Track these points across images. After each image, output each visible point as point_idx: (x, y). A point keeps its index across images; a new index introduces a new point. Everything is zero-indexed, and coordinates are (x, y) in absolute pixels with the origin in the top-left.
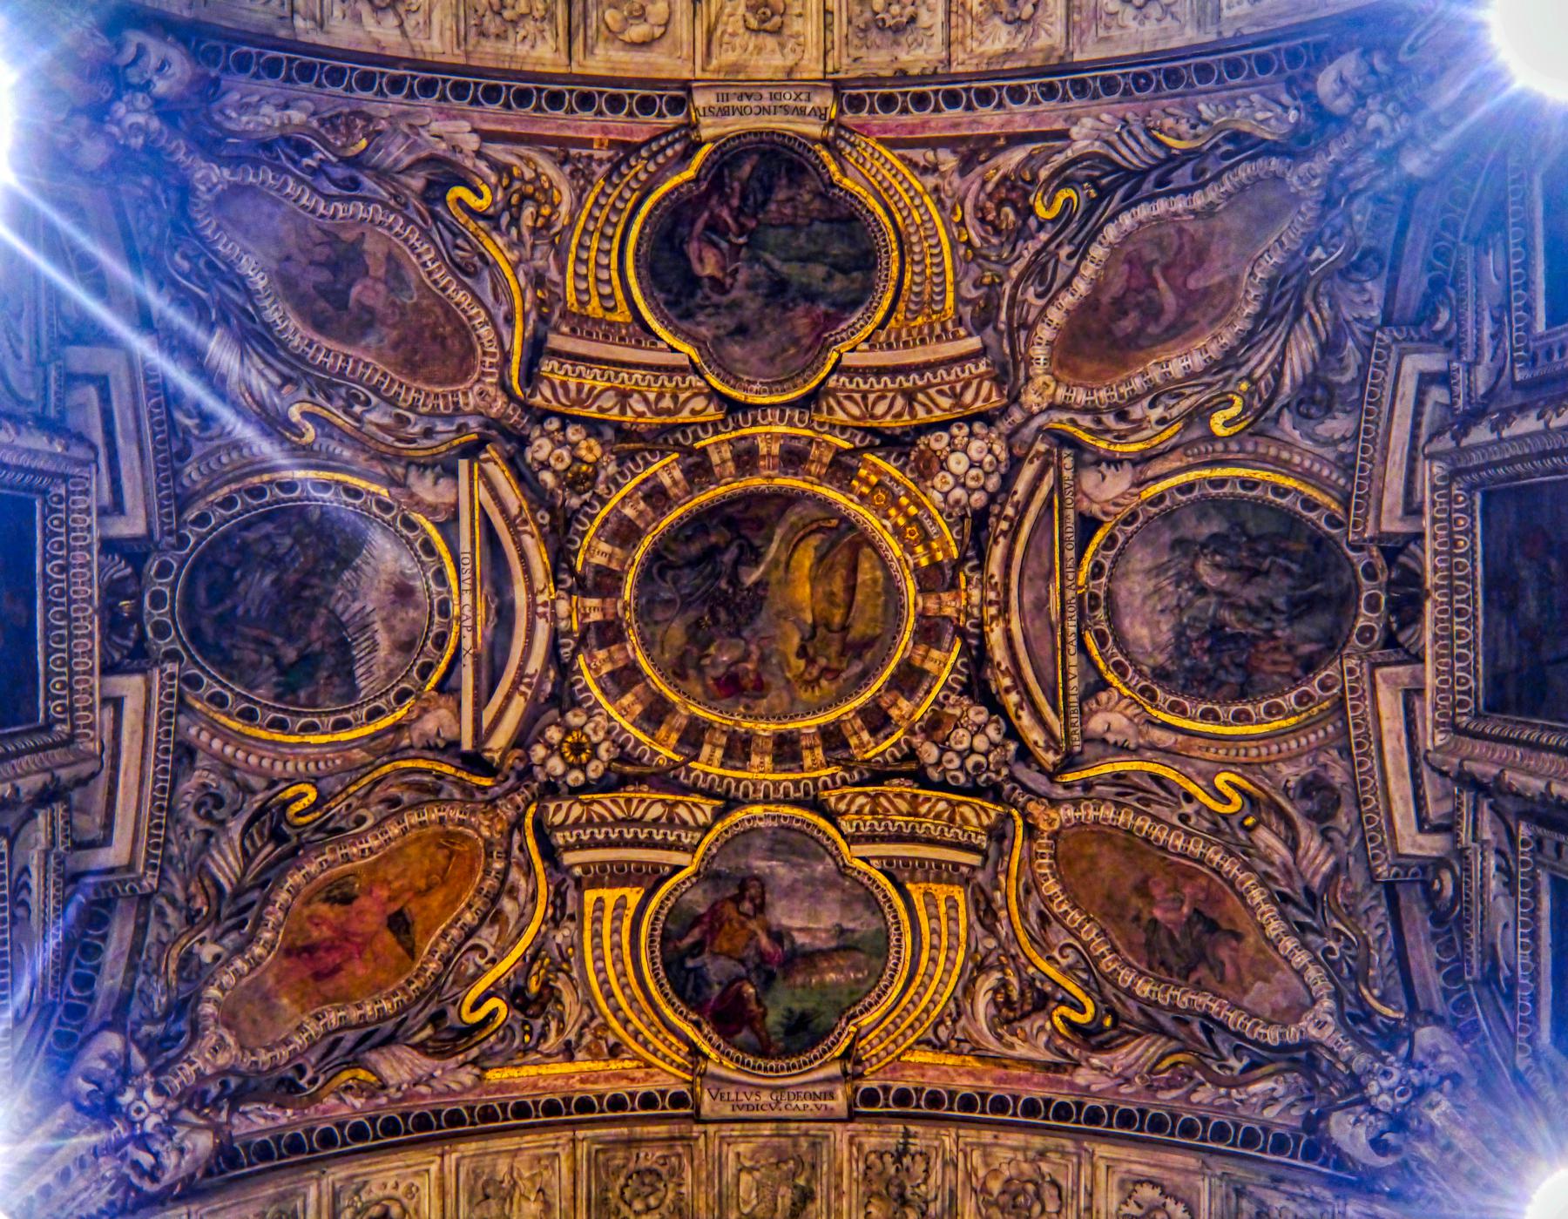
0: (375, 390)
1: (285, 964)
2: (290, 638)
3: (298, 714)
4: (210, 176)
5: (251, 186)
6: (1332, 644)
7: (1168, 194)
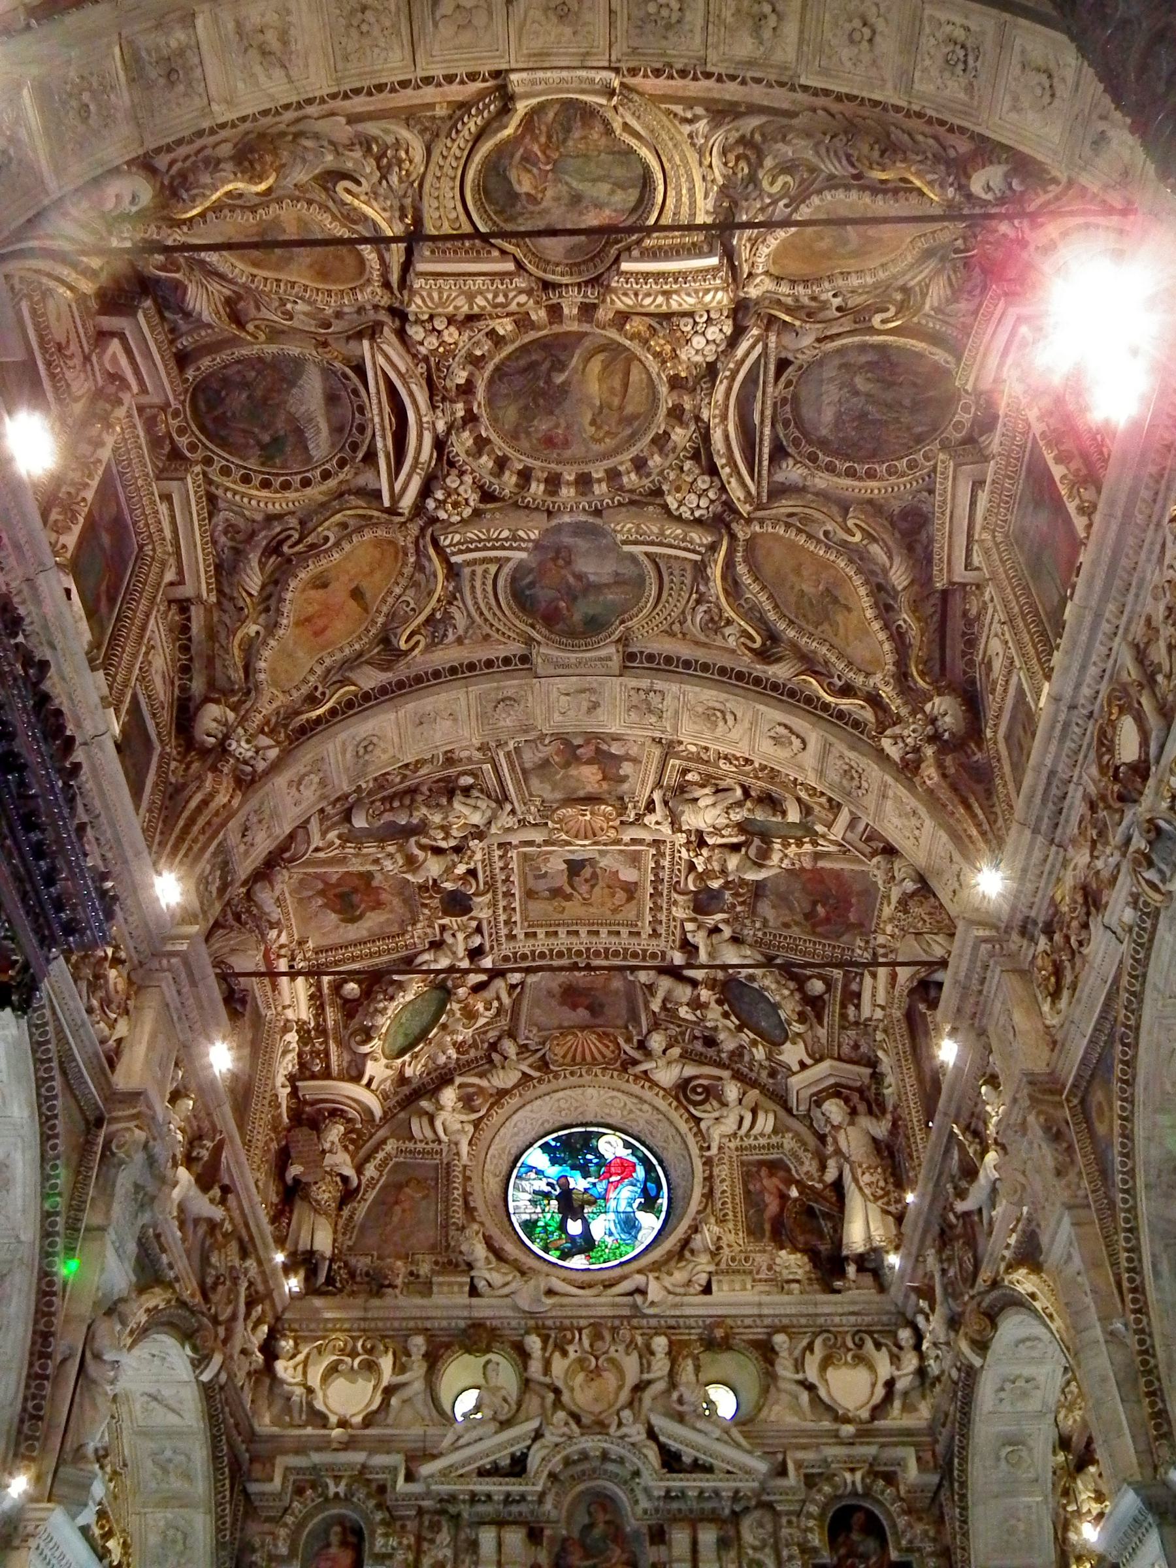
2: (264, 428)
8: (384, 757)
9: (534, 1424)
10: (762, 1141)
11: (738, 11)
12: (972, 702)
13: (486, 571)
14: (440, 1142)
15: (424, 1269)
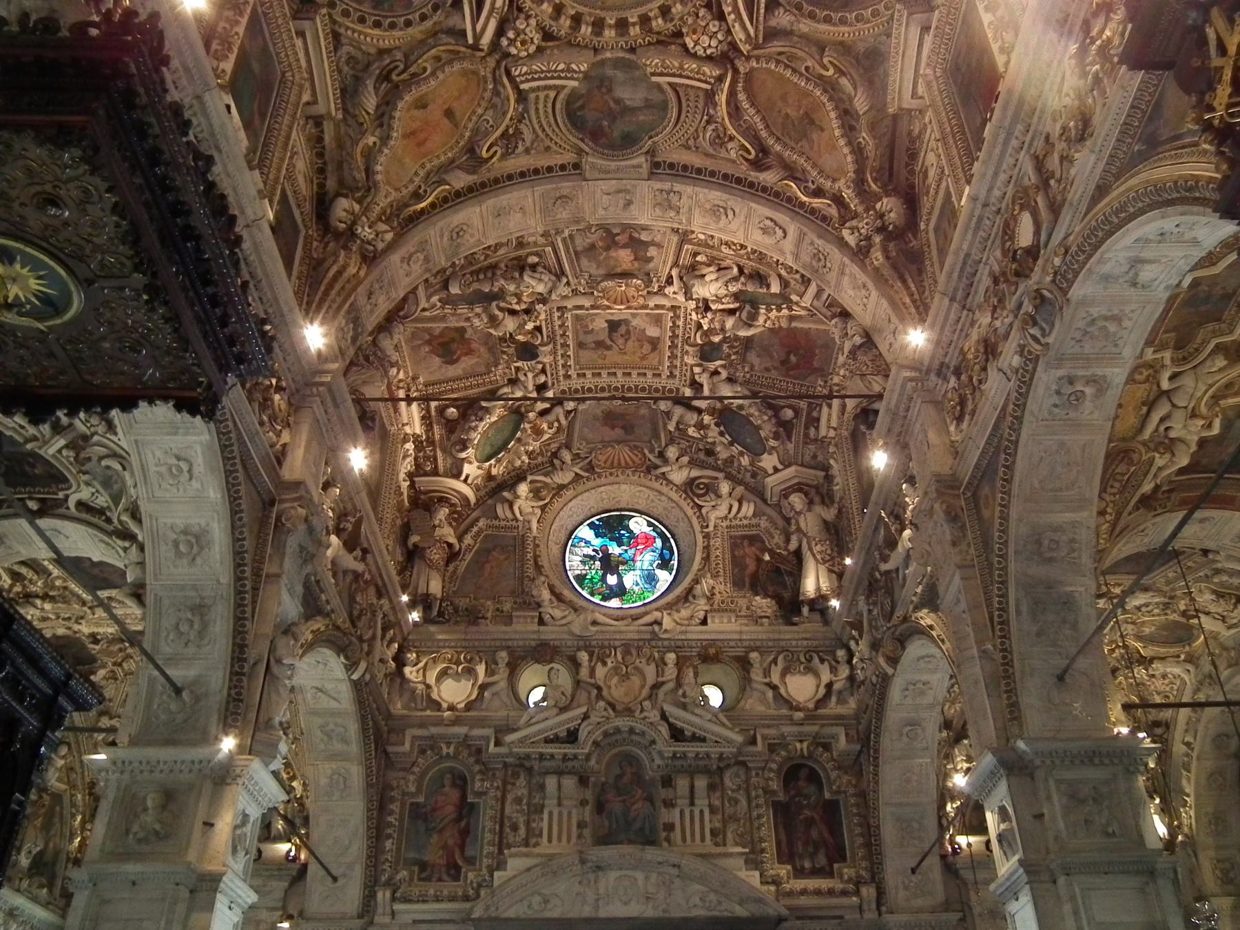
3: (387, 17)
8: (472, 240)
9: (584, 709)
10: (745, 522)
12: (911, 202)
13: (547, 96)
14: (517, 520)
15: (507, 607)
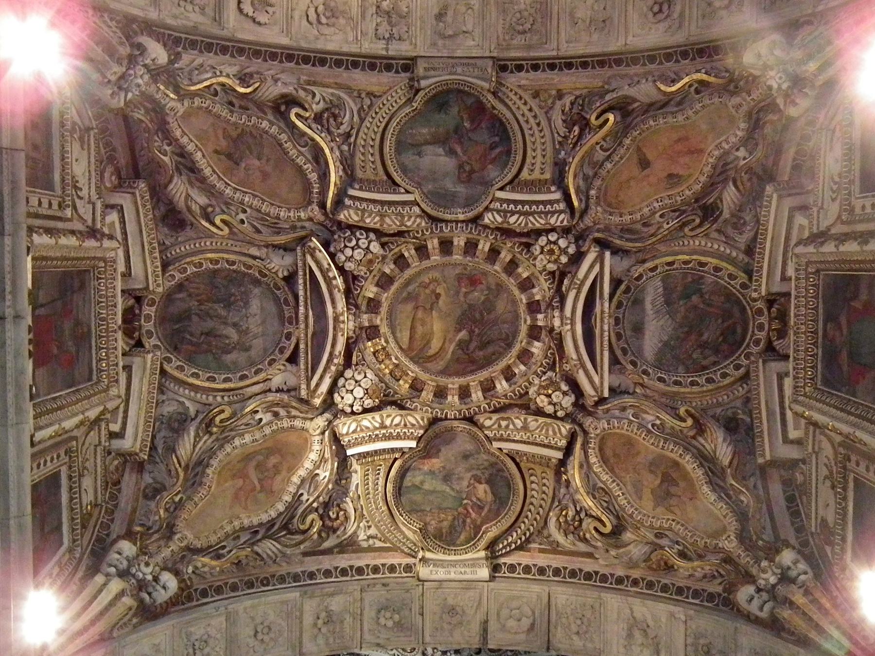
0: (649, 431)
1: (702, 146)
2: (695, 307)
3: (692, 269)
4: (730, 544)
5: (709, 537)
6: (169, 297)
7: (253, 527)
11: (342, 622)
